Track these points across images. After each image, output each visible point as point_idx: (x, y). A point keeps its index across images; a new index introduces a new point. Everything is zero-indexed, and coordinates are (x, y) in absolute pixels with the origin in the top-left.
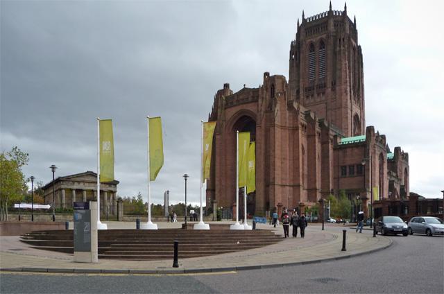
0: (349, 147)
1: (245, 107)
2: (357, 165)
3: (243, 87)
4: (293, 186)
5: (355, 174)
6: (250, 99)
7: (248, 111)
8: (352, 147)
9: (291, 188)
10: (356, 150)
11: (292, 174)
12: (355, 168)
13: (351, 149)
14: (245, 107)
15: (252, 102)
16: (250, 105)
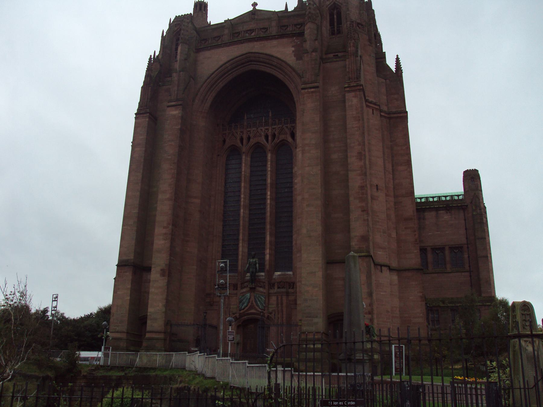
0: (431, 209)
1: (256, 47)
2: (452, 248)
3: (251, 8)
4: (398, 271)
5: (448, 266)
6: (274, 31)
7: (269, 59)
8: (437, 209)
9: (395, 277)
10: (445, 217)
11: (394, 235)
12: (447, 252)
13: (433, 213)
14: (256, 47)
15: (281, 36)
16: (275, 42)
